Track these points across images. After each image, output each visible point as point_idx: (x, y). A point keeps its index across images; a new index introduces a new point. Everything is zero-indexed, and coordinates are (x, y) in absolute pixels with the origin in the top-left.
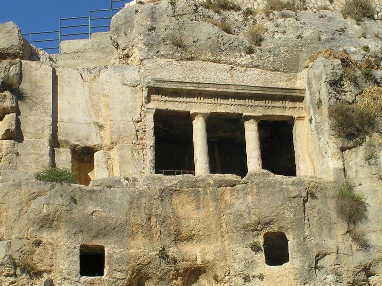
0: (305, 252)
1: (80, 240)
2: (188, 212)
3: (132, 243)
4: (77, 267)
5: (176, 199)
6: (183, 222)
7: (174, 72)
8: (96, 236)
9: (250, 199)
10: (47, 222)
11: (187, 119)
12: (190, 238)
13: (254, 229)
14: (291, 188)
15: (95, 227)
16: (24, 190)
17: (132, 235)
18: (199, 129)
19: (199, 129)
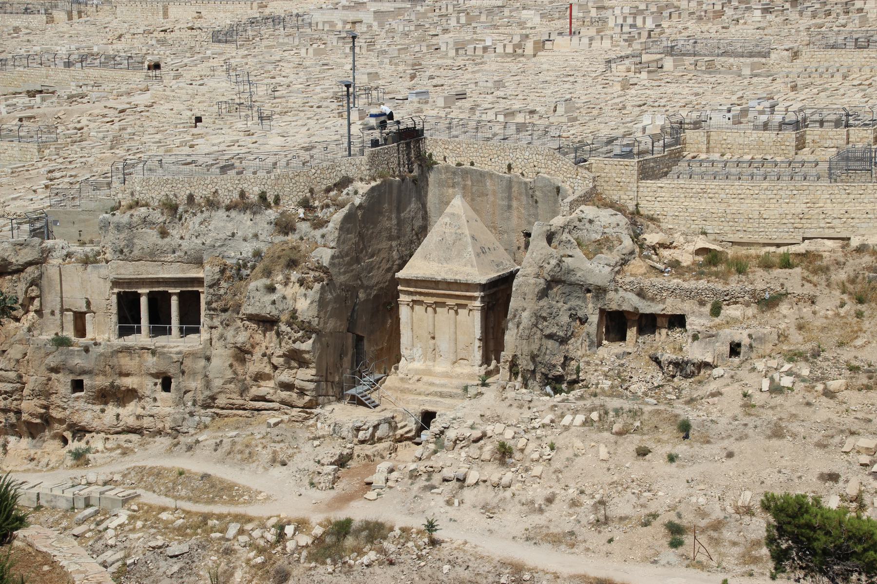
0: (178, 389)
1: (72, 377)
2: (126, 362)
3: (97, 379)
4: (70, 391)
5: (120, 355)
6: (123, 368)
7: (129, 271)
8: (80, 374)
9: (155, 359)
10: (55, 370)
11: (139, 295)
12: (127, 375)
13: (156, 376)
14: (174, 356)
15: (78, 371)
16: (43, 351)
17: (96, 374)
18: (144, 301)
19: (144, 301)
